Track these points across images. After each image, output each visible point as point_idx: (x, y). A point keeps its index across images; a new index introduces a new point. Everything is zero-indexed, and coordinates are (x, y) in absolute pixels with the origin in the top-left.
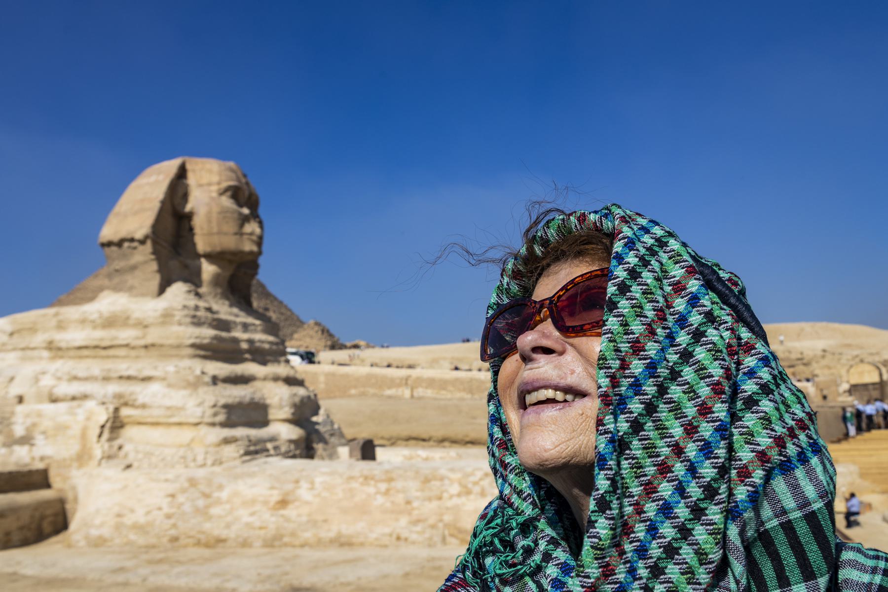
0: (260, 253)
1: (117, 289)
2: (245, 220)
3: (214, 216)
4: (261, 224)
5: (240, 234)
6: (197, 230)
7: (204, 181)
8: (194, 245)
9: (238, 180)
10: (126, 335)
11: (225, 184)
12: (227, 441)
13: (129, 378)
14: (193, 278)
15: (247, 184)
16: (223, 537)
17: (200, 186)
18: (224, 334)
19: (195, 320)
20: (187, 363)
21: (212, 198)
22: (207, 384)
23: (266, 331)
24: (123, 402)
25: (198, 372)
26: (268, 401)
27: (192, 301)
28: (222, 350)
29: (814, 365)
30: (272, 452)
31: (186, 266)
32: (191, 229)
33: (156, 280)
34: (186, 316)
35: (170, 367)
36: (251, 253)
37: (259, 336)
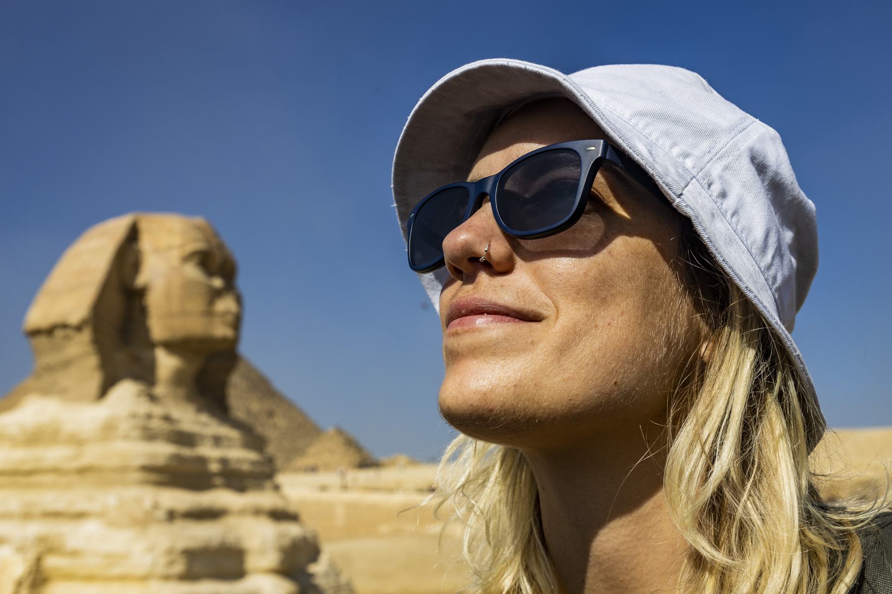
1: (46, 392)
2: (215, 295)
4: (239, 300)
5: (209, 313)
9: (208, 241)
10: (54, 455)
13: (56, 515)
15: (221, 246)
17: (157, 250)
18: (186, 452)
22: (159, 521)
24: (48, 547)
25: (148, 503)
27: (144, 407)
28: (184, 474)
33: (95, 380)
35: (109, 499)
36: (224, 340)
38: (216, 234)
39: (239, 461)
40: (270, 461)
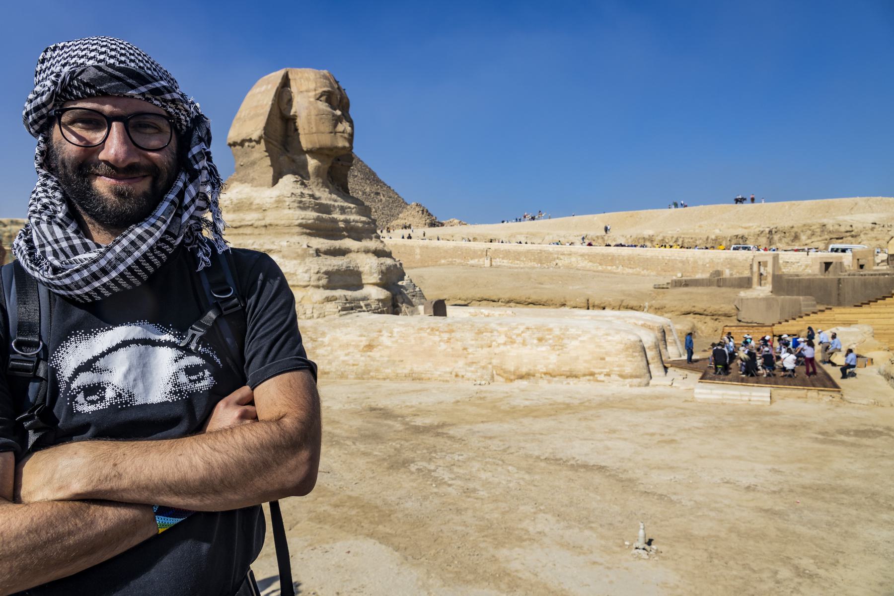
0: (351, 147)
1: (243, 181)
2: (337, 120)
3: (313, 117)
6: (301, 131)
7: (304, 88)
8: (300, 142)
9: (332, 87)
11: (320, 90)
12: (328, 300)
14: (300, 172)
15: (339, 88)
16: (327, 370)
19: (301, 205)
20: (297, 239)
21: (310, 102)
22: (312, 255)
23: (359, 213)
25: (305, 246)
26: (361, 269)
27: (299, 189)
29: (862, 236)
30: (364, 308)
31: (294, 161)
32: (296, 130)
33: (270, 173)
34: (294, 202)
36: (344, 148)
37: (353, 217)
38: (337, 82)
39: (357, 222)
40: (374, 221)
